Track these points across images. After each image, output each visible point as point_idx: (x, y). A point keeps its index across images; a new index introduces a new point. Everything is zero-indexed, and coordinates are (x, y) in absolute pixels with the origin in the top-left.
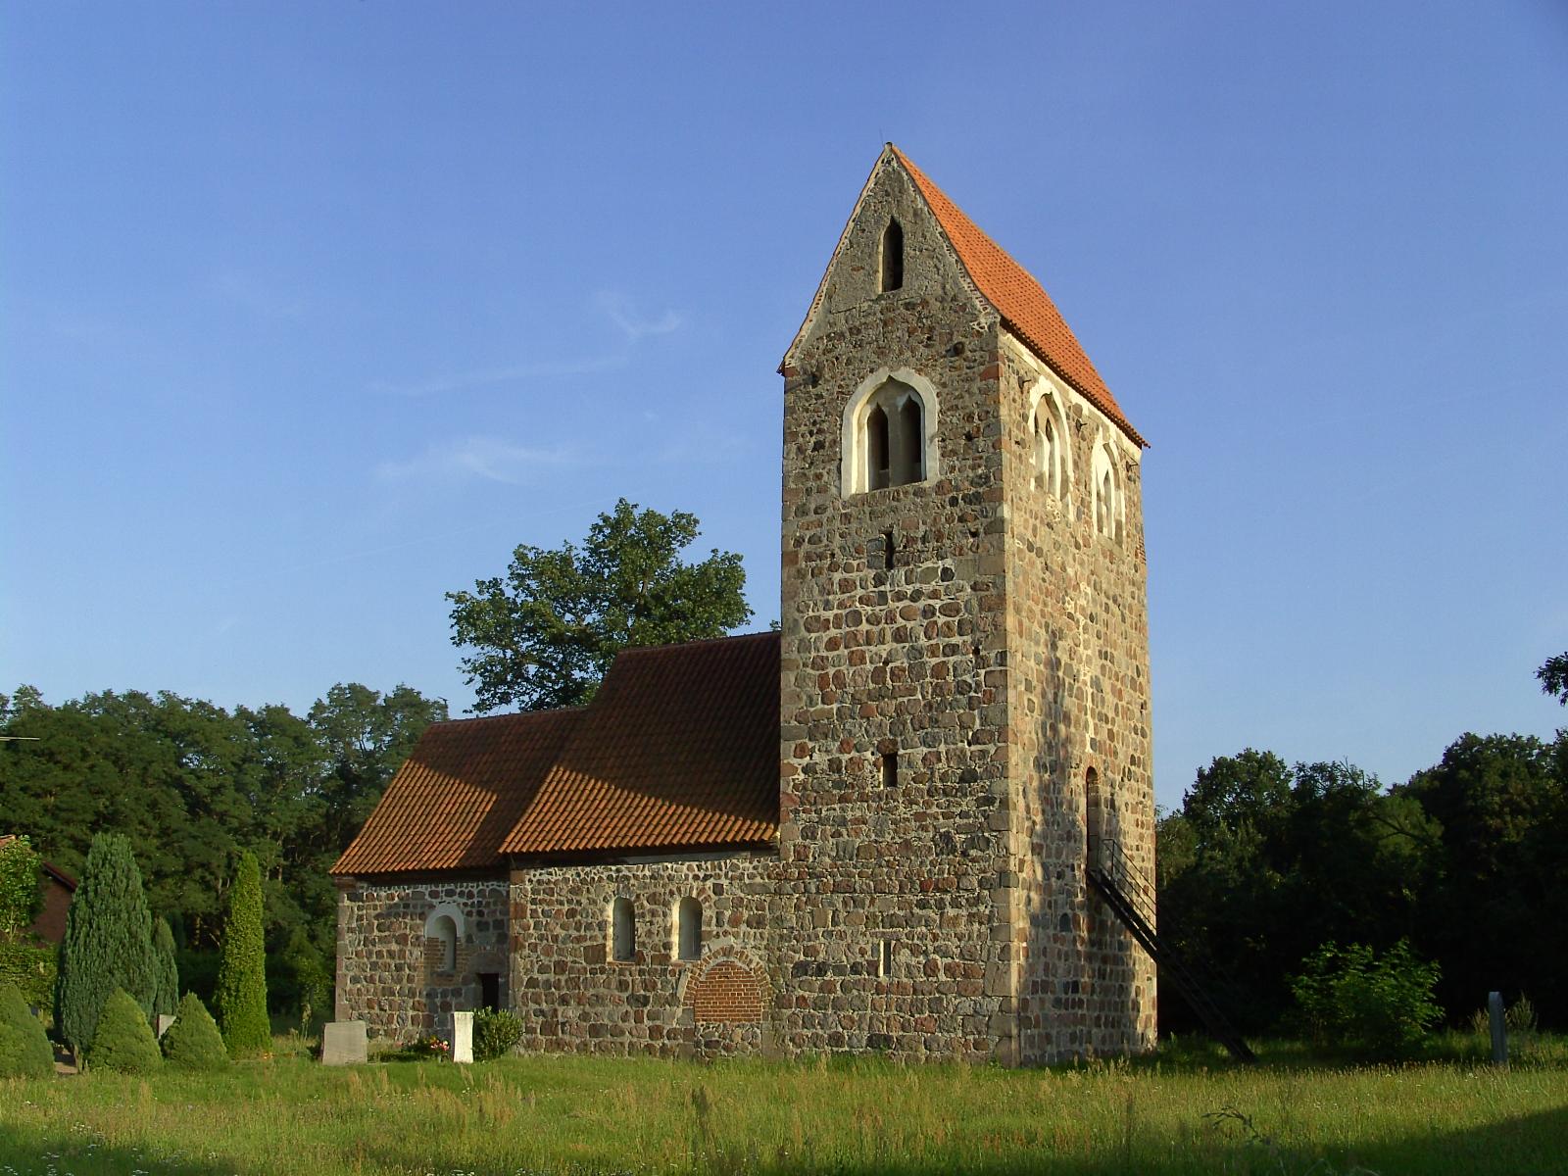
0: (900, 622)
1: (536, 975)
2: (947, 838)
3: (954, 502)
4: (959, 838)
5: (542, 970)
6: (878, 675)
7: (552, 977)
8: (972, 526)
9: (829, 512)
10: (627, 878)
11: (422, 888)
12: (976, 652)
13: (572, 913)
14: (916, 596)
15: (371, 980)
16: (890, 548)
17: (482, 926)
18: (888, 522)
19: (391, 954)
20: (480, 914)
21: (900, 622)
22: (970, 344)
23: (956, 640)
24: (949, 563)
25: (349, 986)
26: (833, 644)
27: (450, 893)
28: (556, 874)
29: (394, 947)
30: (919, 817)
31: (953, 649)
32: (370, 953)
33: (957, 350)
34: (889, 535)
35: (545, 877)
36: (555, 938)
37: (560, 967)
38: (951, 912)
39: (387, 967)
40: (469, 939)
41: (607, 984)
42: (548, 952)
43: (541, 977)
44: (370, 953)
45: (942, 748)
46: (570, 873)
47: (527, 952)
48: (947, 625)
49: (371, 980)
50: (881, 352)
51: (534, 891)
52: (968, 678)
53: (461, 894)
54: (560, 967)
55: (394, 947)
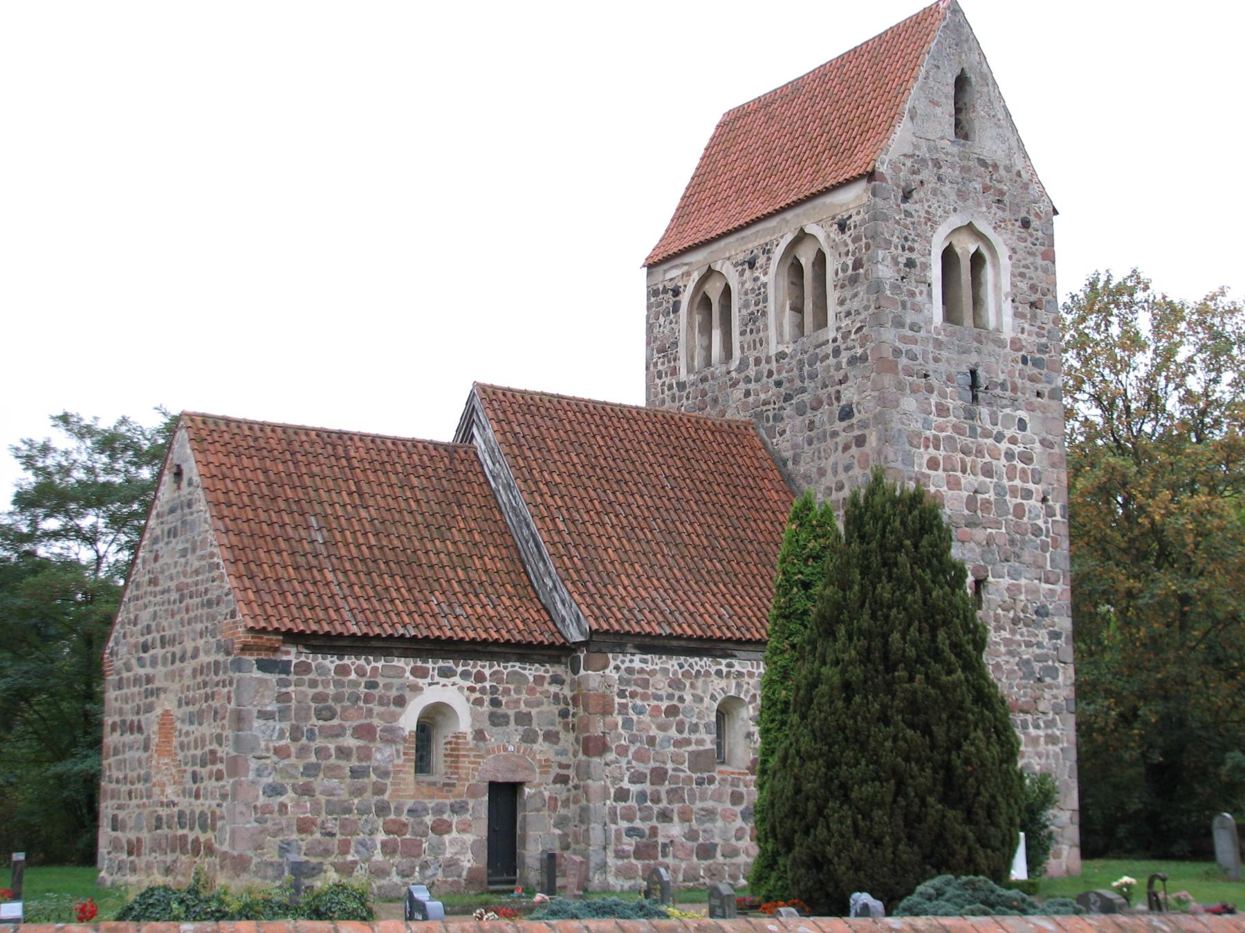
0: (987, 459)
1: (626, 784)
2: (1027, 662)
3: (1024, 360)
4: (1037, 666)
5: (637, 778)
6: (971, 502)
7: (647, 787)
8: (1039, 386)
9: (923, 333)
10: (740, 674)
11: (399, 662)
12: (1044, 500)
13: (672, 711)
14: (999, 438)
15: (307, 791)
16: (974, 385)
17: (497, 720)
18: (973, 358)
19: (343, 753)
20: (495, 703)
21: (987, 459)
22: (1035, 223)
23: (1031, 486)
24: (1022, 414)
25: (262, 800)
26: (933, 464)
27: (446, 673)
28: (655, 663)
29: (350, 742)
30: (1007, 642)
31: (1028, 494)
32: (303, 752)
33: (1026, 224)
34: (973, 373)
35: (637, 665)
36: (651, 741)
37: (659, 775)
38: (1031, 730)
39: (332, 771)
40: (479, 735)
41: (718, 797)
42: (640, 757)
43: (634, 788)
44: (303, 752)
45: (1023, 581)
46: (672, 664)
47: (611, 756)
48: (1023, 471)
49: (307, 791)
50: (962, 195)
51: (621, 680)
52: (1040, 522)
53: (465, 675)
54: (659, 775)
55: (350, 742)
